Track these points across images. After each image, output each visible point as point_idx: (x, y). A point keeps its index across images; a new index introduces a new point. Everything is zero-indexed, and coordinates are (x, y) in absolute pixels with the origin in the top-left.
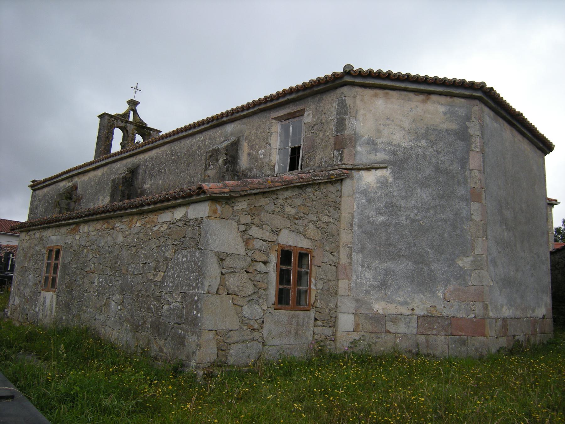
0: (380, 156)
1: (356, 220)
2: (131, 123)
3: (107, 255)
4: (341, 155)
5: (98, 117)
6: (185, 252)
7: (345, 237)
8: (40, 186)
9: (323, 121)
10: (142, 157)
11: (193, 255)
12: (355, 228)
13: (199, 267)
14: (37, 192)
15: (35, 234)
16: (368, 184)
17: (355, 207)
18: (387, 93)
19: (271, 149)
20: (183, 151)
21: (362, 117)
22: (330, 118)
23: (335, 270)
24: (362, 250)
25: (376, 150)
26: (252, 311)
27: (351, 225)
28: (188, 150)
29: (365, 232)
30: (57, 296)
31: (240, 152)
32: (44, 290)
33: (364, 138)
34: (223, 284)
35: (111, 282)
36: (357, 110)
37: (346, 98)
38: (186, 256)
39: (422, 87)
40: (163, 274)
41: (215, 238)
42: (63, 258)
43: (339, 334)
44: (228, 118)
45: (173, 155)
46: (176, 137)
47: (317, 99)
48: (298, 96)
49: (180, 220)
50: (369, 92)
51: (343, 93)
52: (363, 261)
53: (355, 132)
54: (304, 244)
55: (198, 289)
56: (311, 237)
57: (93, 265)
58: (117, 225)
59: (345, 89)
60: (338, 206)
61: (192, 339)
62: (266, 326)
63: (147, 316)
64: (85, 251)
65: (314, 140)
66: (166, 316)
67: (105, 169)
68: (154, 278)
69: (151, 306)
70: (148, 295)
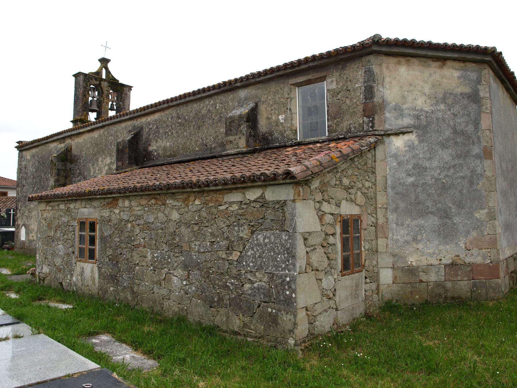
0: (407, 121)
1: (389, 182)
2: (105, 80)
3: (160, 231)
4: (372, 122)
5: (74, 76)
6: (268, 233)
7: (381, 199)
8: (28, 147)
9: (349, 88)
10: (143, 120)
11: (279, 237)
12: (389, 190)
13: (288, 249)
14: (24, 153)
15: (58, 205)
16: (397, 148)
17: (388, 170)
18: (408, 60)
19: (292, 114)
20: (191, 114)
21: (388, 84)
22: (357, 85)
23: (374, 230)
24: (396, 210)
25: (402, 115)
26: (328, 282)
27: (386, 188)
28: (196, 114)
29: (397, 193)
30: (99, 268)
31: (258, 117)
32: (80, 261)
33: (391, 105)
34: (308, 264)
35: (169, 257)
36: (383, 78)
37: (373, 66)
38: (269, 238)
39: (440, 54)
40: (239, 254)
41: (300, 219)
42: (101, 230)
43: (381, 287)
44: (242, 84)
45: (179, 118)
46: (183, 101)
47: (341, 66)
48: (320, 64)
49: (254, 201)
50: (392, 60)
51: (369, 61)
52: (397, 219)
53: (383, 99)
54: (355, 210)
55: (289, 271)
56: (359, 204)
57: (142, 240)
58: (168, 202)
59: (372, 58)
60: (374, 171)
61: (286, 318)
62: (338, 293)
63: (223, 294)
64: (129, 225)
65: (340, 107)
66: (250, 295)
67: (102, 131)
68: (228, 257)
69: (228, 284)
70: (222, 273)
